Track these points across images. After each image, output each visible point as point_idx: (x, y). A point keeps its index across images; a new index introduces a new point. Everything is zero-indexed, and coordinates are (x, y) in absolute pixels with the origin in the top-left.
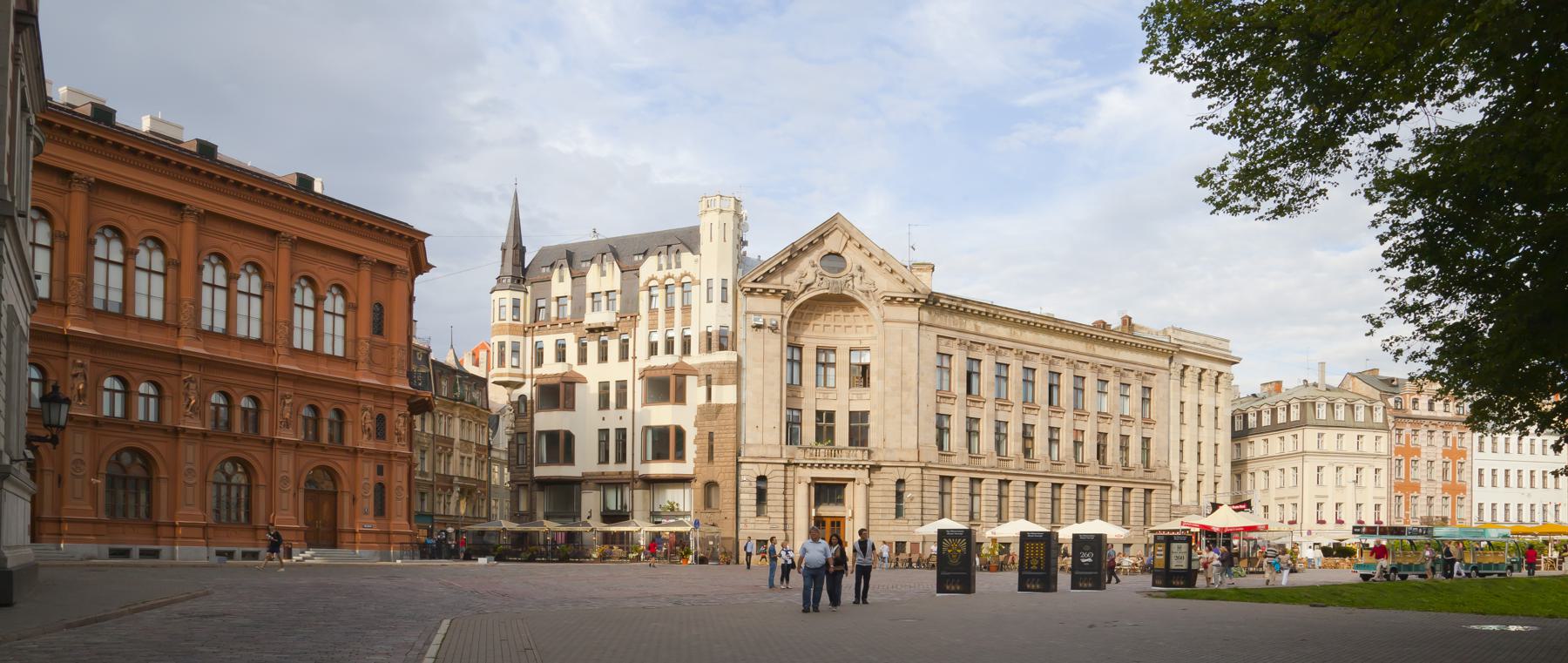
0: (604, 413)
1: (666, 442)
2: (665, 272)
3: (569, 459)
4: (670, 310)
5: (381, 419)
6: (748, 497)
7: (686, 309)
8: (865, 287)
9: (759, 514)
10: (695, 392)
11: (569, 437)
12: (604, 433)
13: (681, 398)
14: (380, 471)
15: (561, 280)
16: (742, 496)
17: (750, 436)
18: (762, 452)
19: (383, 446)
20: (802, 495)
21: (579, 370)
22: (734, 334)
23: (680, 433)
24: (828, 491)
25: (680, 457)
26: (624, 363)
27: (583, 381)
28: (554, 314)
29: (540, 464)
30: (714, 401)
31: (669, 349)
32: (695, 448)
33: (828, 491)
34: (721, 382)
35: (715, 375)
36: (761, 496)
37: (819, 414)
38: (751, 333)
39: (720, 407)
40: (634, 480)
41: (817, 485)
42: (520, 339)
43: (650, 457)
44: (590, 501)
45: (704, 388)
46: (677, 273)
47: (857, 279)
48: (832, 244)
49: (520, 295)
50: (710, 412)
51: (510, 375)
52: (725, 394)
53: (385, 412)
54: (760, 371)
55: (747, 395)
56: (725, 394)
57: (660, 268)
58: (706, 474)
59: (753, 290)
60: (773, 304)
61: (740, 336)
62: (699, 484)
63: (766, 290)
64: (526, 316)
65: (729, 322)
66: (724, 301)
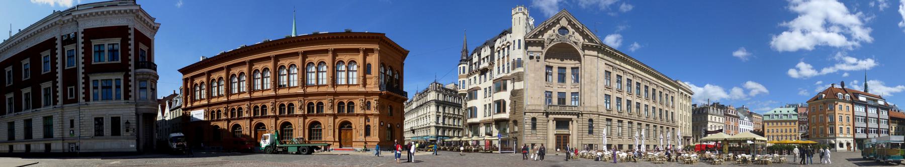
3: (476, 117)
6: (528, 126)
7: (508, 56)
11: (475, 108)
12: (485, 105)
13: (505, 88)
20: (552, 125)
23: (504, 102)
24: (562, 124)
25: (504, 111)
27: (480, 89)
33: (562, 124)
34: (520, 80)
35: (516, 77)
36: (534, 126)
50: (514, 93)
52: (518, 86)
54: (533, 75)
56: (518, 86)
58: (514, 118)
60: (539, 49)
64: (467, 72)
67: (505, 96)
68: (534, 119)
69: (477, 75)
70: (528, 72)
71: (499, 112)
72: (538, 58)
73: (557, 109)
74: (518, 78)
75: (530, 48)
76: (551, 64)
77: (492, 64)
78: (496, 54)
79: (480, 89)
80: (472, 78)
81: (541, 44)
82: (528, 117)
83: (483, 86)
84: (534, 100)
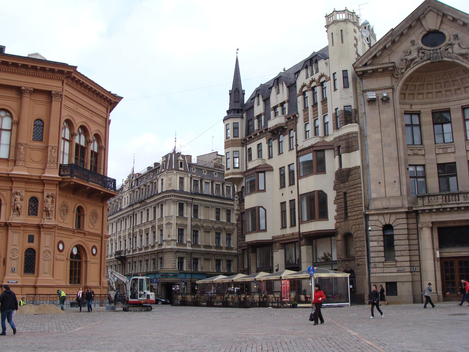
0: (283, 190)
1: (316, 204)
2: (310, 79)
4: (315, 105)
5: (34, 200)
6: (376, 245)
7: (324, 101)
8: (463, 51)
9: (387, 258)
10: (331, 162)
12: (283, 204)
14: (31, 239)
15: (258, 104)
16: (371, 244)
17: (375, 191)
18: (385, 204)
19: (34, 220)
21: (269, 162)
22: (356, 111)
23: (322, 196)
25: (324, 215)
26: (292, 151)
27: (270, 169)
28: (256, 127)
29: (250, 233)
30: (344, 167)
31: (316, 134)
32: (335, 207)
34: (350, 149)
37: (440, 166)
38: (368, 108)
39: (349, 170)
40: (301, 239)
41: (439, 229)
42: (239, 149)
43: (305, 218)
44: (278, 257)
45: (337, 157)
46: (316, 77)
47: (456, 47)
48: (431, 23)
49: (238, 120)
51: (233, 174)
52: (352, 160)
53: (39, 196)
54: (378, 136)
55: (371, 157)
56: (352, 160)
57: (307, 77)
59: (364, 72)
60: (386, 81)
61: (361, 111)
62: (339, 237)
63: (374, 71)
64: (242, 134)
65: (351, 102)
66: (346, 86)
67: (324, 182)
68: (387, 228)
69: (263, 141)
70: (368, 131)
71: (311, 218)
72: (386, 100)
73: (438, 202)
74: (347, 145)
75: (367, 83)
76: (415, 108)
77: (292, 119)
78: (300, 99)
79: (270, 169)
80: (253, 146)
81: (391, 71)
82: (375, 226)
83: (277, 162)
84: (385, 187)
